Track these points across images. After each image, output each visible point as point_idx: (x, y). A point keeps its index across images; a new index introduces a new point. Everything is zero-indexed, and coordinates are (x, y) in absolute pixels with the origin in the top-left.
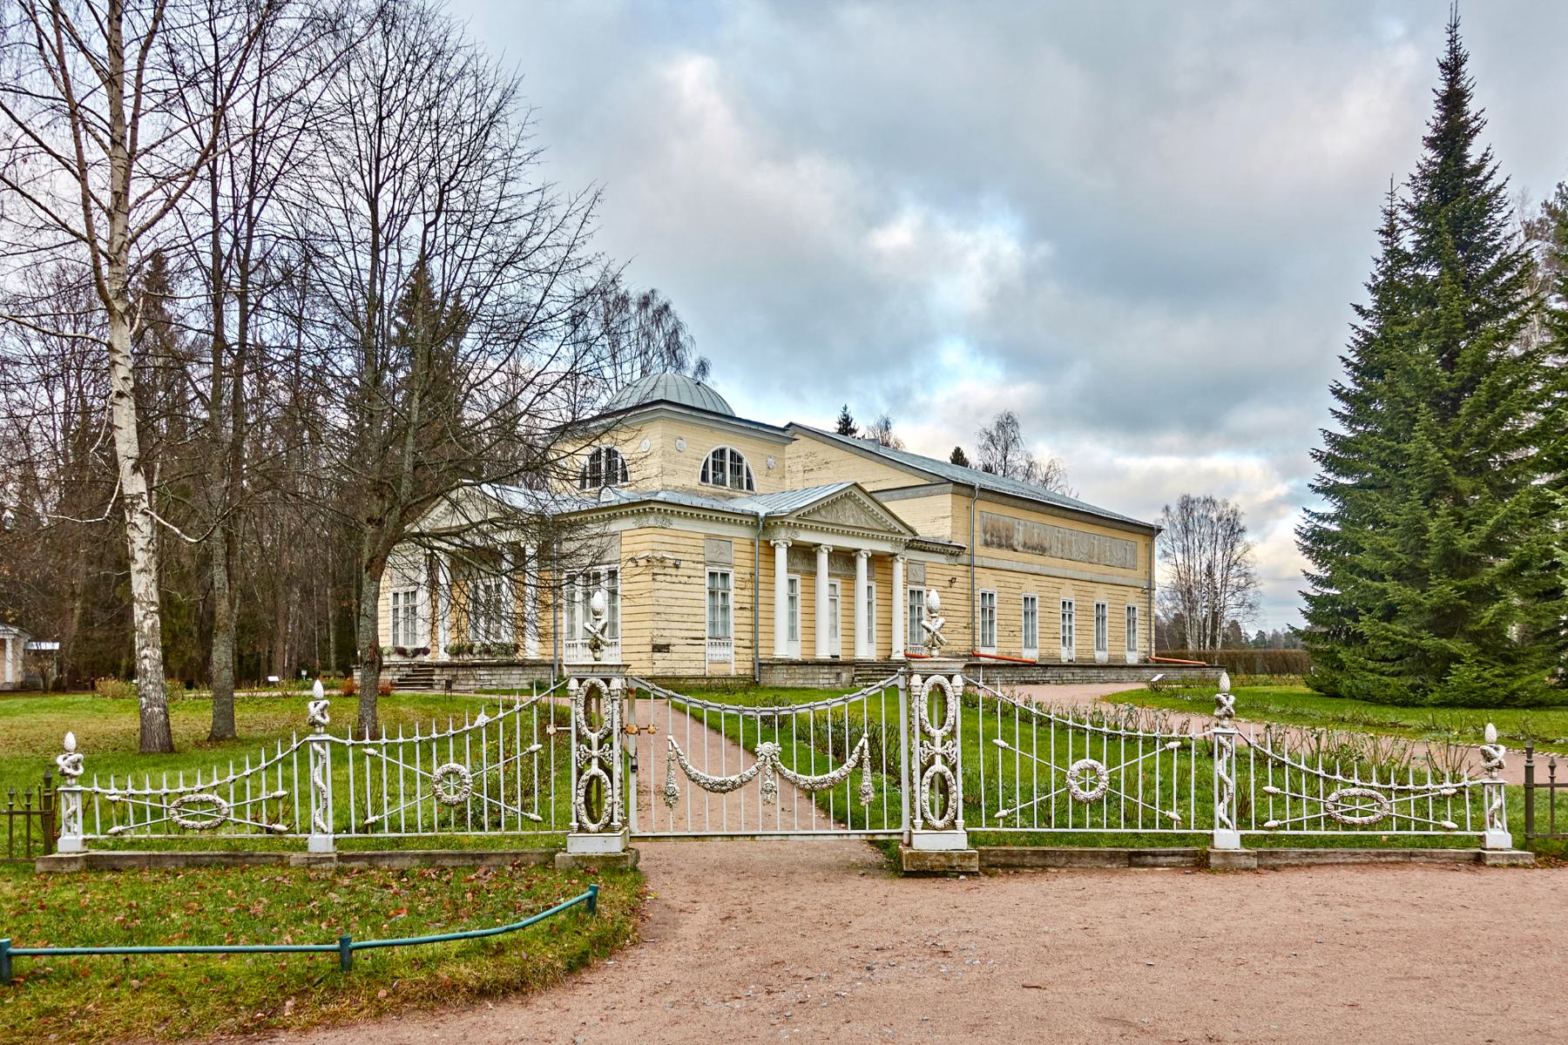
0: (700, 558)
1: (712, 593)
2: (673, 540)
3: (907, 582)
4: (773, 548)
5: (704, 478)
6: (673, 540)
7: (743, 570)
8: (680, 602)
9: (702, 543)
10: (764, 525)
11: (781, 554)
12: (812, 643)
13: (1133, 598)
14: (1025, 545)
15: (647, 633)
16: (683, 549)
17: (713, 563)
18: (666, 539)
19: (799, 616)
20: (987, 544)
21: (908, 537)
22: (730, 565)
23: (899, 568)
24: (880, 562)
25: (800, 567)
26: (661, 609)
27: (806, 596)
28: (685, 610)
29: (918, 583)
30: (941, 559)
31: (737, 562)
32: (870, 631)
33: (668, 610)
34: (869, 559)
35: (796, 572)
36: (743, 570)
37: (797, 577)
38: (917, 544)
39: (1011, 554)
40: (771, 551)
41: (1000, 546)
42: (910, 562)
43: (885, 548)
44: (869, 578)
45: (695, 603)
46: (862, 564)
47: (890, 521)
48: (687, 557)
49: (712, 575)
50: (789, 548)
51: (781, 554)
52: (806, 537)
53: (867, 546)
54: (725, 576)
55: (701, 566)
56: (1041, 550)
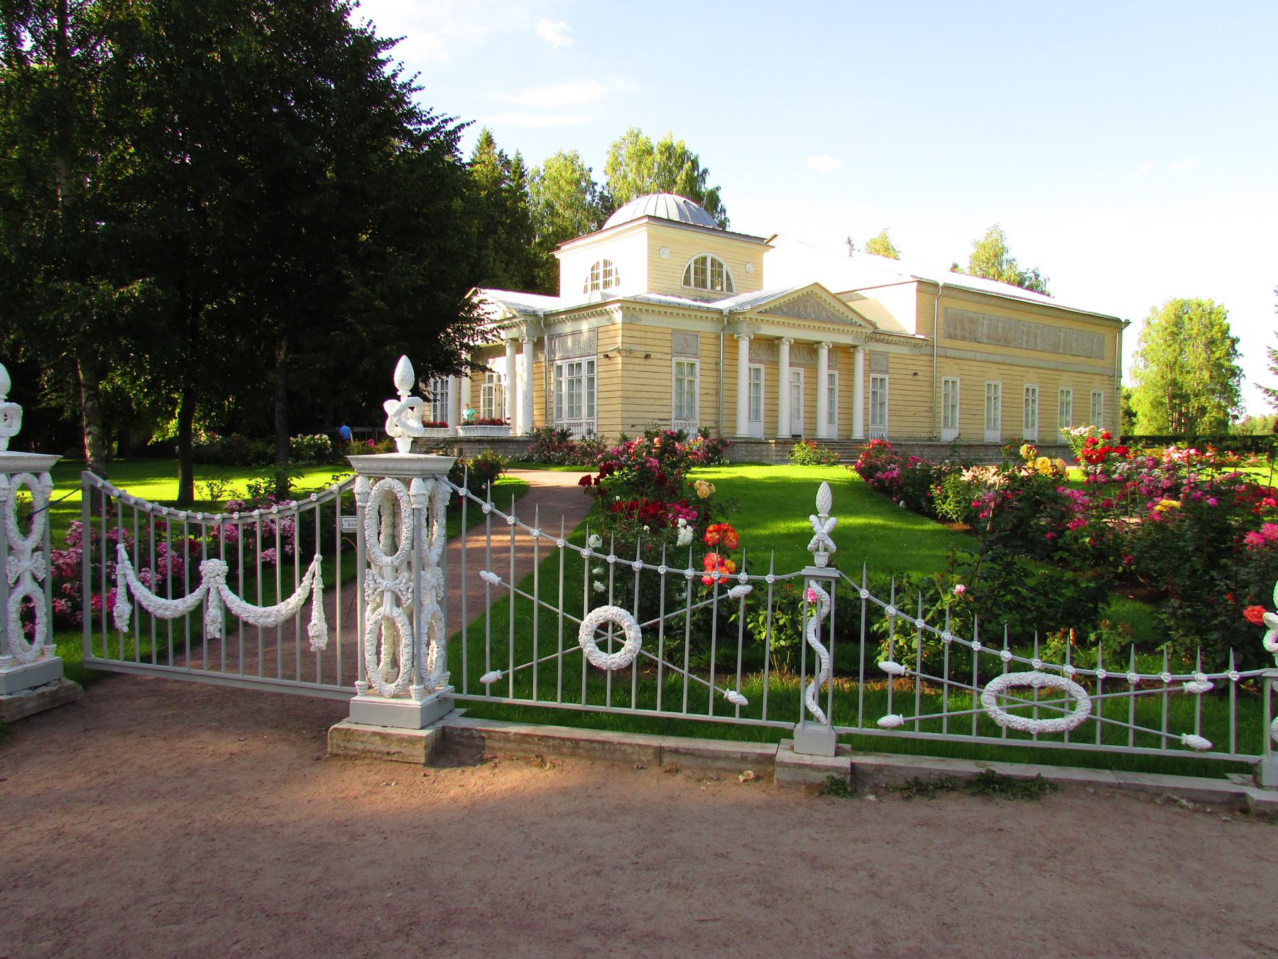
0: (668, 350)
1: (680, 381)
2: (642, 335)
3: (866, 374)
4: (737, 341)
5: (687, 282)
6: (642, 335)
7: (709, 360)
8: (646, 388)
9: (669, 337)
10: (730, 320)
11: (744, 346)
12: (773, 423)
13: (1099, 386)
14: (989, 337)
15: (618, 414)
16: (650, 342)
17: (680, 353)
18: (636, 334)
19: (762, 401)
20: (950, 337)
21: (870, 330)
22: (696, 355)
23: (860, 358)
24: (843, 353)
25: (763, 358)
26: (629, 394)
27: (769, 383)
28: (652, 395)
29: (880, 372)
30: (905, 350)
31: (704, 353)
32: (831, 415)
33: (637, 395)
34: (829, 351)
35: (760, 362)
36: (709, 360)
37: (762, 367)
38: (878, 335)
39: (974, 345)
40: (733, 344)
41: (963, 339)
42: (872, 353)
43: (846, 340)
44: (829, 367)
45: (662, 389)
46: (824, 354)
47: (851, 316)
48: (655, 349)
49: (679, 364)
50: (751, 343)
51: (744, 346)
52: (768, 331)
53: (828, 337)
54: (693, 365)
55: (668, 357)
56: (1007, 343)
